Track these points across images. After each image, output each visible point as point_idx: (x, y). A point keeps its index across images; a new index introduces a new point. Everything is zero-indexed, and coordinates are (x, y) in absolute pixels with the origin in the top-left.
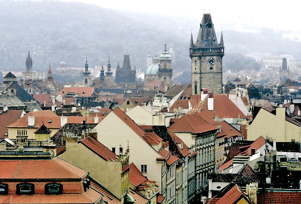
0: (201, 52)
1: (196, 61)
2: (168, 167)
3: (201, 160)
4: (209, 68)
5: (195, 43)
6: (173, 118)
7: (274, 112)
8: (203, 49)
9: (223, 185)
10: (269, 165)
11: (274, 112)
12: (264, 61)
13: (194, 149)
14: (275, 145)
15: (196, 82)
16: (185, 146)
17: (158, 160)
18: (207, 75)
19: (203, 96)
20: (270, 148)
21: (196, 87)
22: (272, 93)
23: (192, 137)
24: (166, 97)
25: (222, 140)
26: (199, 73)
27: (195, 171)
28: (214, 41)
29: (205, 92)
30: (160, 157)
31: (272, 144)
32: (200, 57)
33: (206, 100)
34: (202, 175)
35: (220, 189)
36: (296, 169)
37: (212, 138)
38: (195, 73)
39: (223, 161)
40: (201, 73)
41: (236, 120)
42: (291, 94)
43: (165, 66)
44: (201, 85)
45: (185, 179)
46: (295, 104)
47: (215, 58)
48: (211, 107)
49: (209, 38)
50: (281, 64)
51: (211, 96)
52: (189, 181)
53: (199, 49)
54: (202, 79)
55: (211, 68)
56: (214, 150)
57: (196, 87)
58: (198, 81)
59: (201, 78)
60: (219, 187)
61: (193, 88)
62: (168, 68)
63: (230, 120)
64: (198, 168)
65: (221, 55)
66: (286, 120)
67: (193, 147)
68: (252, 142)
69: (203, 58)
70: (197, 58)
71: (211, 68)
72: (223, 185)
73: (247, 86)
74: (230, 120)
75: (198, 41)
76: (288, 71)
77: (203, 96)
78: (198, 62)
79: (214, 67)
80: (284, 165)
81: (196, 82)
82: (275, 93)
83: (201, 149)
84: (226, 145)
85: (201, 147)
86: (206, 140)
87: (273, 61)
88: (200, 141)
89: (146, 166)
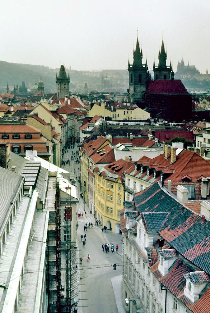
0: (60, 80)
2: (62, 127)
3: (70, 125)
4: (64, 87)
5: (58, 77)
6: (58, 107)
7: (100, 105)
8: (62, 80)
9: (89, 135)
10: (105, 126)
11: (100, 105)
12: (76, 84)
13: (67, 120)
14: (104, 118)
15: (59, 93)
17: (59, 125)
18: (63, 90)
19: (66, 99)
20: (103, 120)
22: (87, 97)
23: (66, 115)
24: (46, 99)
25: (76, 117)
29: (67, 97)
30: (60, 123)
31: (103, 118)
32: (60, 83)
33: (67, 101)
35: (88, 137)
36: (115, 128)
37: (73, 116)
38: (59, 89)
39: (80, 126)
40: (61, 89)
41: (80, 109)
42: (95, 97)
43: (41, 86)
44: (61, 93)
46: (107, 102)
47: (66, 83)
48: (69, 103)
50: (85, 85)
51: (69, 99)
53: (60, 79)
55: (65, 87)
56: (74, 121)
58: (60, 92)
59: (61, 91)
60: (86, 136)
61: (58, 95)
62: (42, 86)
63: (78, 109)
64: (68, 128)
65: (69, 82)
66: (105, 108)
67: (66, 119)
68: (92, 117)
69: (61, 83)
70: (59, 83)
71: (65, 87)
72: (89, 135)
73: (77, 95)
74: (78, 109)
75: (59, 76)
76: (87, 88)
77: (66, 99)
78: (60, 85)
79: (66, 87)
80: (110, 126)
81: (59, 93)
82: (89, 97)
84: (78, 119)
86: (71, 116)
87: (80, 84)
88: (69, 117)
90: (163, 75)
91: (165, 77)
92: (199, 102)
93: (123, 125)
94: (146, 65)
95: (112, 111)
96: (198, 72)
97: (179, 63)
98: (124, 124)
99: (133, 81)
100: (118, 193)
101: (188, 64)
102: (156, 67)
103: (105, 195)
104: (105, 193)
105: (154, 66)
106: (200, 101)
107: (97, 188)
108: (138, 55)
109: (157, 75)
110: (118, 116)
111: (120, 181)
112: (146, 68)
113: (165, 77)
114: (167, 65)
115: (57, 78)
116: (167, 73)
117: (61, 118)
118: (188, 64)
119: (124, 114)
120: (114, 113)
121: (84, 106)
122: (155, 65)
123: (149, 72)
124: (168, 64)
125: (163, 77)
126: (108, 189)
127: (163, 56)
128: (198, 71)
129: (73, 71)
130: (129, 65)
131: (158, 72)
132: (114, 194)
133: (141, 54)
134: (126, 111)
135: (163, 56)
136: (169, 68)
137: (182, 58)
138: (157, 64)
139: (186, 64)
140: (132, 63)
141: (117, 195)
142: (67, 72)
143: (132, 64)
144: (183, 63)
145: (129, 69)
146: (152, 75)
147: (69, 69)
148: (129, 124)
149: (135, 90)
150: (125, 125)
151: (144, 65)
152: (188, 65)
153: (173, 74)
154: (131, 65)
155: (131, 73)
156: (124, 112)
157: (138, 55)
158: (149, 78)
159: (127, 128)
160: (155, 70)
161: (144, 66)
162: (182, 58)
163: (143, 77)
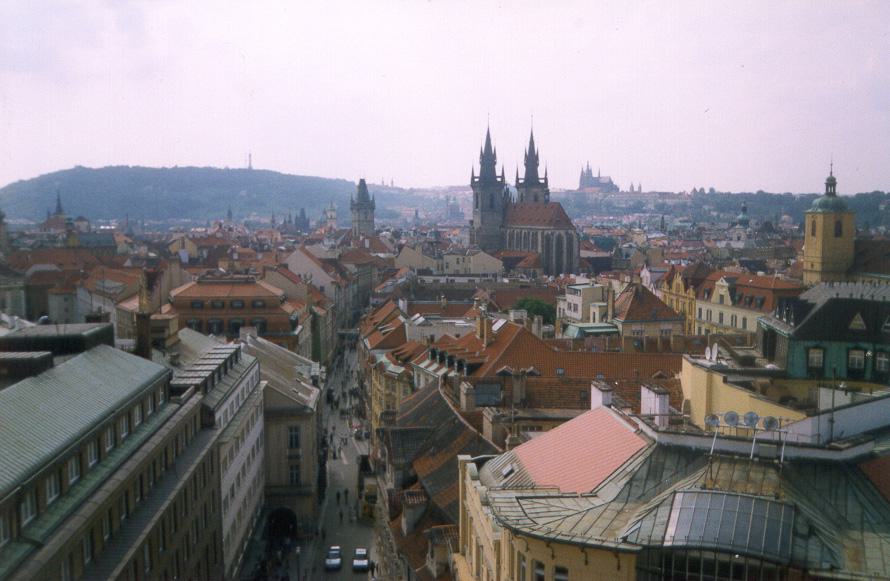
16: (350, 273)
17: (332, 283)
30: (333, 280)
94: (503, 177)
96: (616, 189)
102: (521, 181)
105: (518, 179)
108: (488, 158)
110: (447, 267)
111: (405, 379)
112: (503, 183)
115: (352, 201)
117: (342, 272)
119: (458, 263)
120: (440, 261)
123: (508, 189)
124: (541, 174)
126: (387, 392)
127: (532, 160)
129: (397, 189)
130: (473, 178)
133: (494, 157)
134: (461, 258)
135: (532, 160)
136: (542, 181)
138: (522, 175)
139: (595, 175)
140: (477, 173)
142: (370, 191)
144: (589, 172)
145: (473, 185)
146: (514, 193)
147: (390, 185)
153: (547, 192)
157: (488, 158)
160: (518, 186)
161: (499, 179)
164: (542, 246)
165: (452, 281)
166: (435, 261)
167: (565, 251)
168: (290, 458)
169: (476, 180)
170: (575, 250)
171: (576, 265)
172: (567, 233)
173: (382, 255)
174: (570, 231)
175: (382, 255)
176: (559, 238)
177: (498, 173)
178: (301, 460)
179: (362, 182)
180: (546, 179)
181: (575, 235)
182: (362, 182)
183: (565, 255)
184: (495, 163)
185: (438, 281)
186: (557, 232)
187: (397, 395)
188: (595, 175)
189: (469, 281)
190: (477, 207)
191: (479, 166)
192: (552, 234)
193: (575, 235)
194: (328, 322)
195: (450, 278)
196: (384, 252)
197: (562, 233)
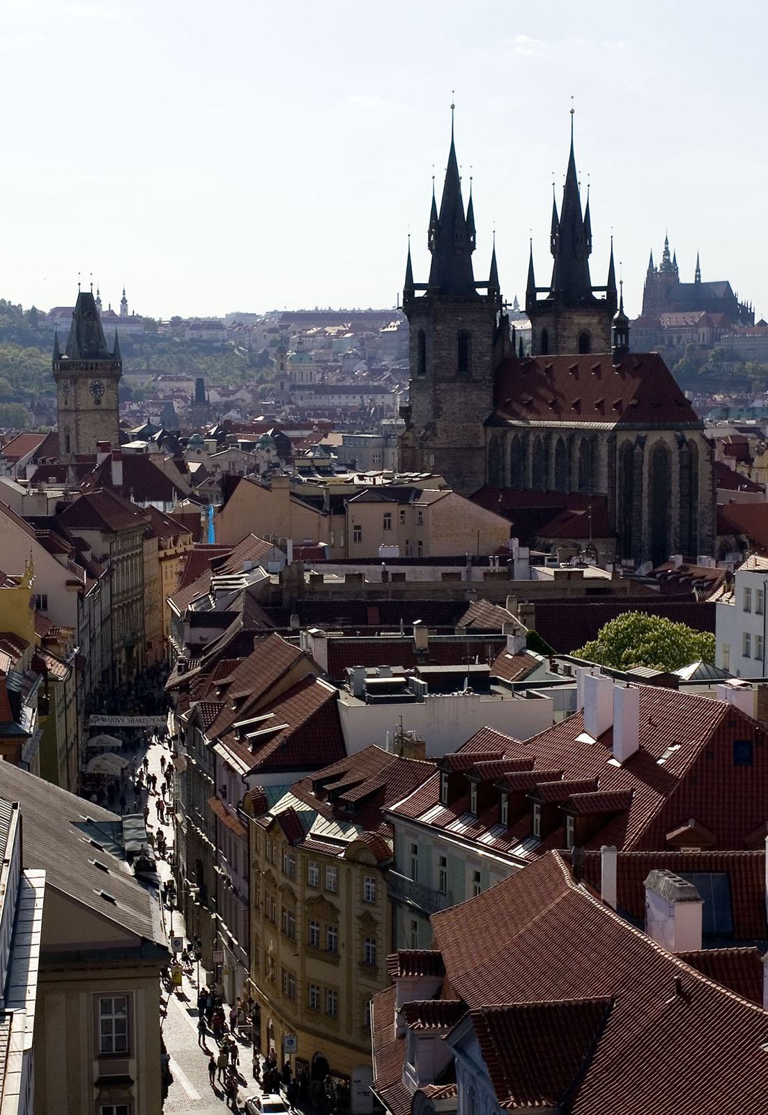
1: (66, 387)
2: (81, 597)
17: (69, 583)
21: (68, 438)
26: (73, 411)
27: (111, 605)
28: (102, 347)
34: (123, 611)
45: (98, 621)
49: (92, 342)
52: (102, 623)
54: (79, 423)
55: (98, 402)
57: (68, 438)
59: (77, 421)
61: (62, 439)
71: (98, 402)
83: (118, 559)
85: (120, 557)
89: (45, 597)
90: (576, 330)
91: (584, 343)
92: (749, 461)
93: (380, 578)
94: (493, 283)
95: (327, 514)
97: (651, 270)
98: (385, 573)
99: (431, 362)
100: (360, 912)
101: (698, 276)
102: (542, 296)
103: (299, 928)
104: (299, 912)
105: (532, 290)
106: (752, 453)
107: (261, 890)
109: (545, 334)
110: (358, 538)
113: (584, 343)
114: (594, 284)
116: (595, 320)
118: (698, 276)
119: (387, 525)
121: (187, 490)
122: (537, 285)
124: (598, 277)
125: (574, 344)
128: (744, 308)
129: (136, 320)
130: (410, 286)
131: (546, 321)
132: (342, 918)
133: (468, 227)
134: (393, 508)
137: (667, 243)
138: (544, 278)
139: (686, 276)
140: (422, 275)
141: (356, 925)
143: (426, 280)
144: (670, 267)
147: (118, 312)
148: (408, 578)
149: (437, 411)
150: (390, 576)
151: (482, 285)
152: (698, 282)
154: (420, 287)
155: (417, 327)
156: (388, 515)
158: (507, 349)
159: (398, 593)
160: (534, 308)
161: (483, 292)
162: (667, 243)
163: (482, 342)
164: (612, 477)
165: (399, 577)
166: (326, 521)
167: (675, 488)
168: (103, 1083)
169: (419, 293)
170: (704, 484)
171: (705, 529)
172: (681, 442)
173: (159, 505)
174: (689, 435)
175: (159, 505)
176: (661, 454)
177: (481, 273)
178: (134, 1090)
179: (87, 302)
180: (611, 288)
181: (702, 447)
182: (87, 302)
183: (675, 500)
184: (472, 247)
185: (360, 576)
186: (653, 438)
187: (340, 902)
188: (686, 276)
189: (446, 576)
190: (422, 370)
191: (428, 256)
192: (641, 442)
193: (702, 447)
194: (70, 696)
195: (392, 569)
196: (167, 498)
197: (668, 437)
